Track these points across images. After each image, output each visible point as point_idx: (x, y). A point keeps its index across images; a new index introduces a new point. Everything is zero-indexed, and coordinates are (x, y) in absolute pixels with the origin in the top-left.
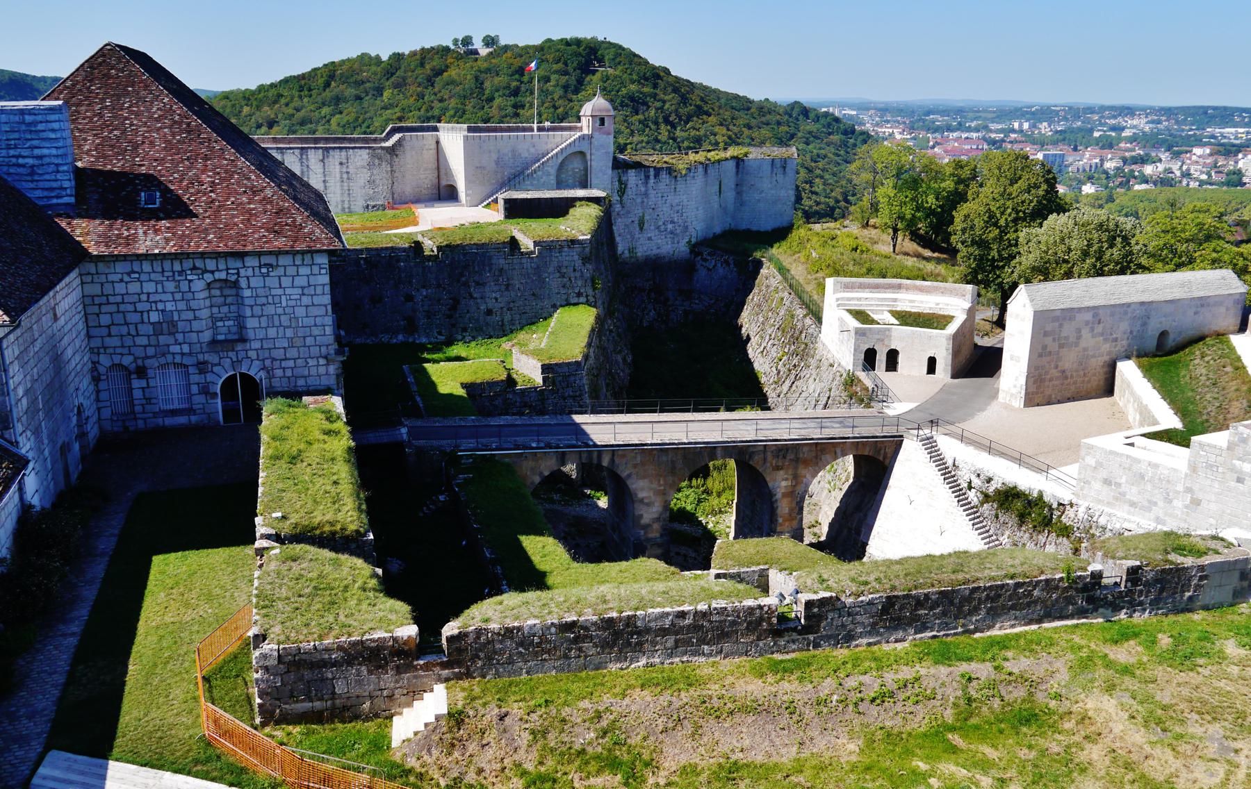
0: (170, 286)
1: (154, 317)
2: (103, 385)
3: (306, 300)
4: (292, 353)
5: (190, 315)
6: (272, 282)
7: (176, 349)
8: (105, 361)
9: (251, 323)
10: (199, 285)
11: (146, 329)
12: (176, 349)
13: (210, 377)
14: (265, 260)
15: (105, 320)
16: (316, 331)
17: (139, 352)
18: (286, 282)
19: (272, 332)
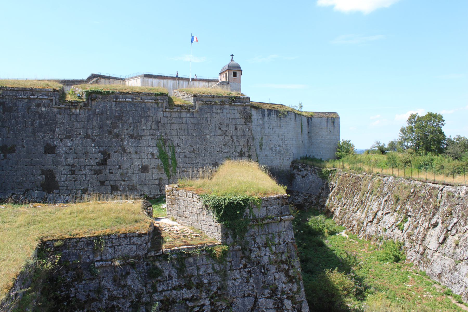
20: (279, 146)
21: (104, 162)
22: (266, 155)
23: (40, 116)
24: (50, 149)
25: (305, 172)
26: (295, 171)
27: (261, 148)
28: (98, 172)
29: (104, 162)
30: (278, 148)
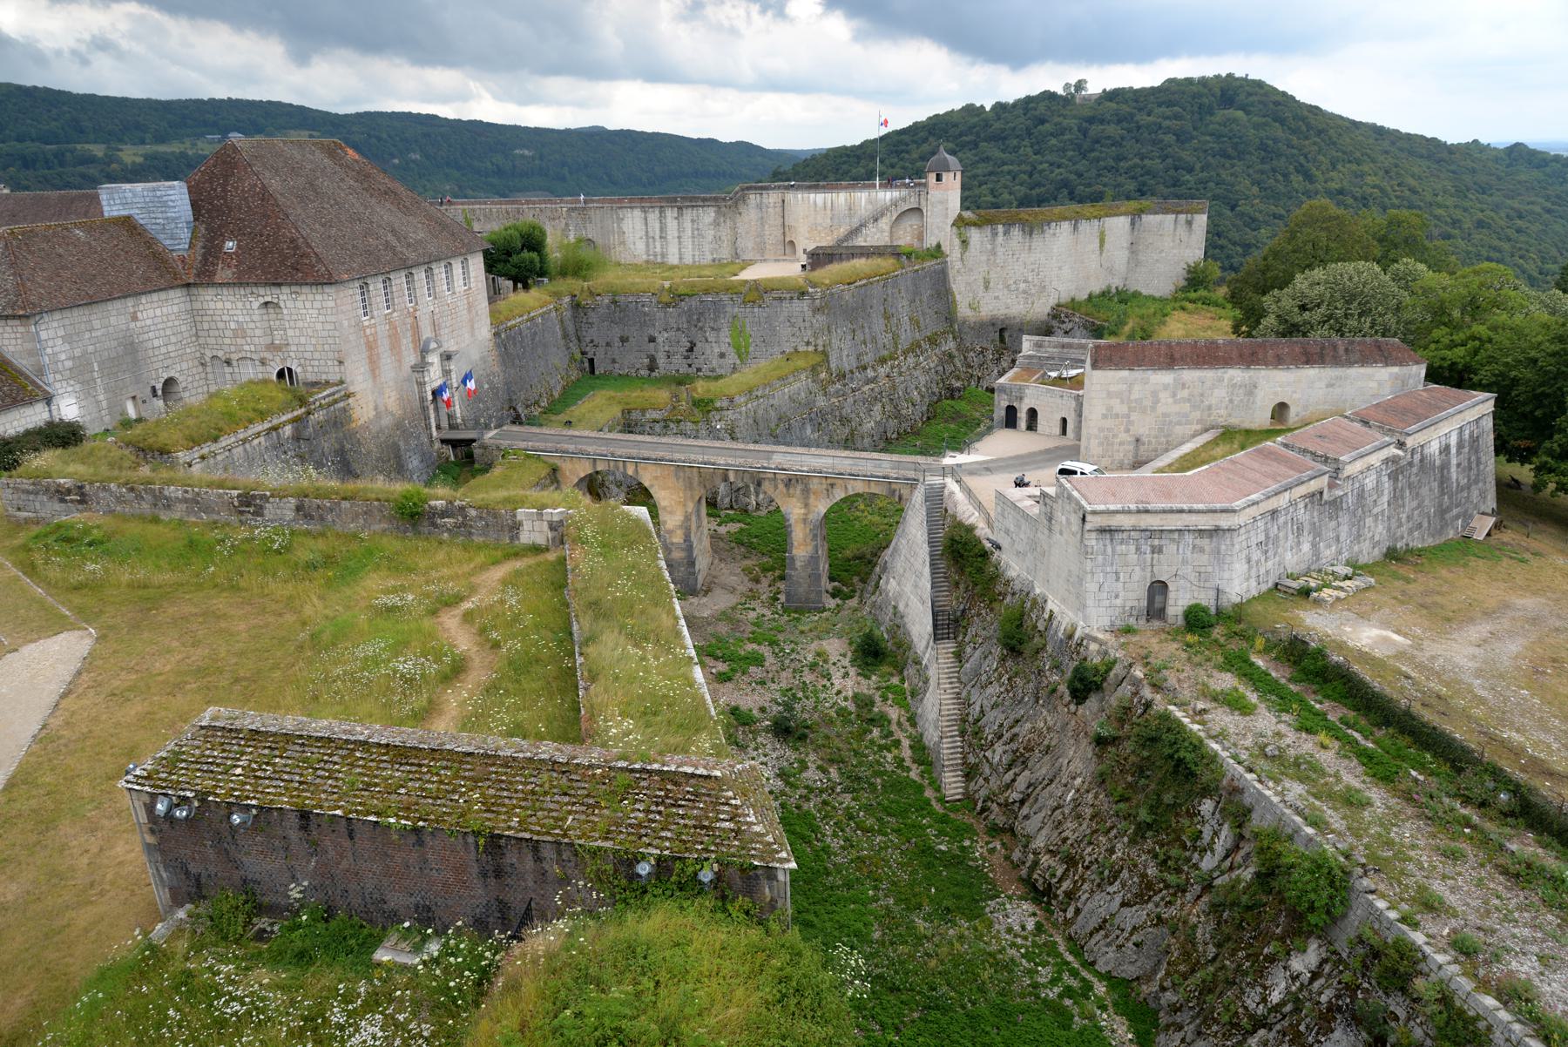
0: (240, 305)
1: (233, 326)
2: (209, 369)
3: (321, 318)
4: (317, 355)
5: (252, 325)
6: (299, 304)
7: (247, 348)
8: (209, 354)
9: (290, 333)
10: (256, 305)
11: (229, 333)
12: (247, 348)
13: (269, 369)
14: (294, 288)
15: (206, 326)
16: (330, 341)
17: (226, 348)
18: (308, 305)
19: (303, 340)
20: (1026, 281)
21: (691, 350)
22: (997, 298)
23: (645, 314)
24: (652, 340)
25: (1070, 326)
26: (1055, 323)
27: (987, 288)
28: (687, 358)
29: (691, 350)
30: (1023, 286)
